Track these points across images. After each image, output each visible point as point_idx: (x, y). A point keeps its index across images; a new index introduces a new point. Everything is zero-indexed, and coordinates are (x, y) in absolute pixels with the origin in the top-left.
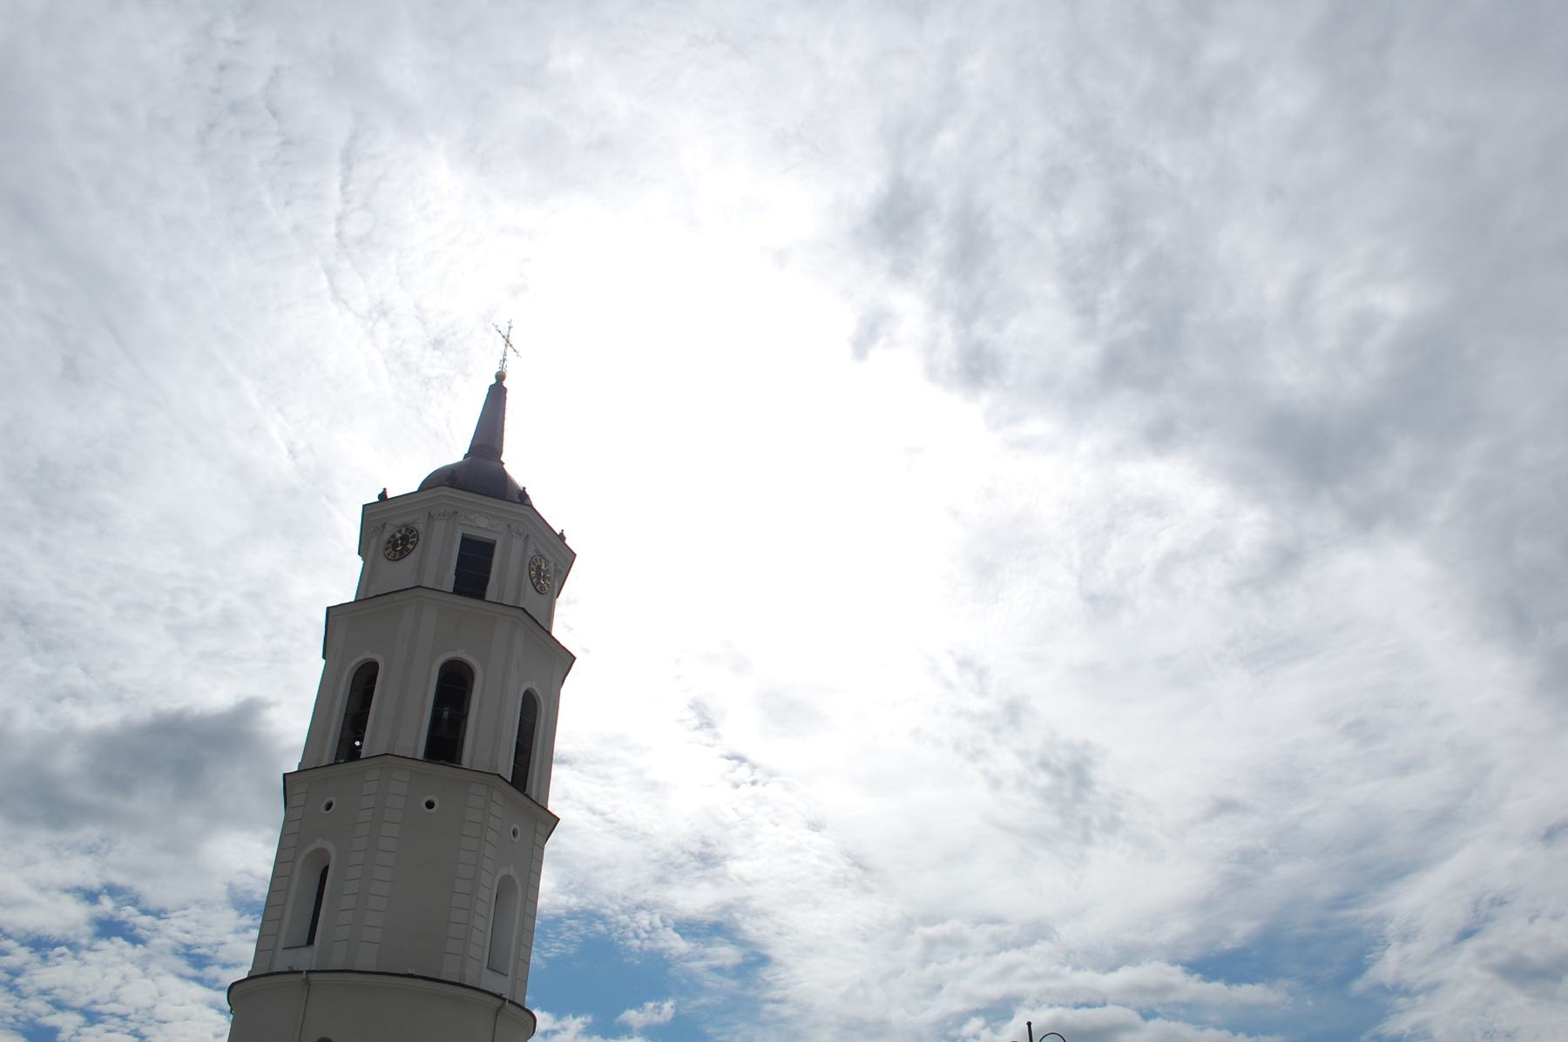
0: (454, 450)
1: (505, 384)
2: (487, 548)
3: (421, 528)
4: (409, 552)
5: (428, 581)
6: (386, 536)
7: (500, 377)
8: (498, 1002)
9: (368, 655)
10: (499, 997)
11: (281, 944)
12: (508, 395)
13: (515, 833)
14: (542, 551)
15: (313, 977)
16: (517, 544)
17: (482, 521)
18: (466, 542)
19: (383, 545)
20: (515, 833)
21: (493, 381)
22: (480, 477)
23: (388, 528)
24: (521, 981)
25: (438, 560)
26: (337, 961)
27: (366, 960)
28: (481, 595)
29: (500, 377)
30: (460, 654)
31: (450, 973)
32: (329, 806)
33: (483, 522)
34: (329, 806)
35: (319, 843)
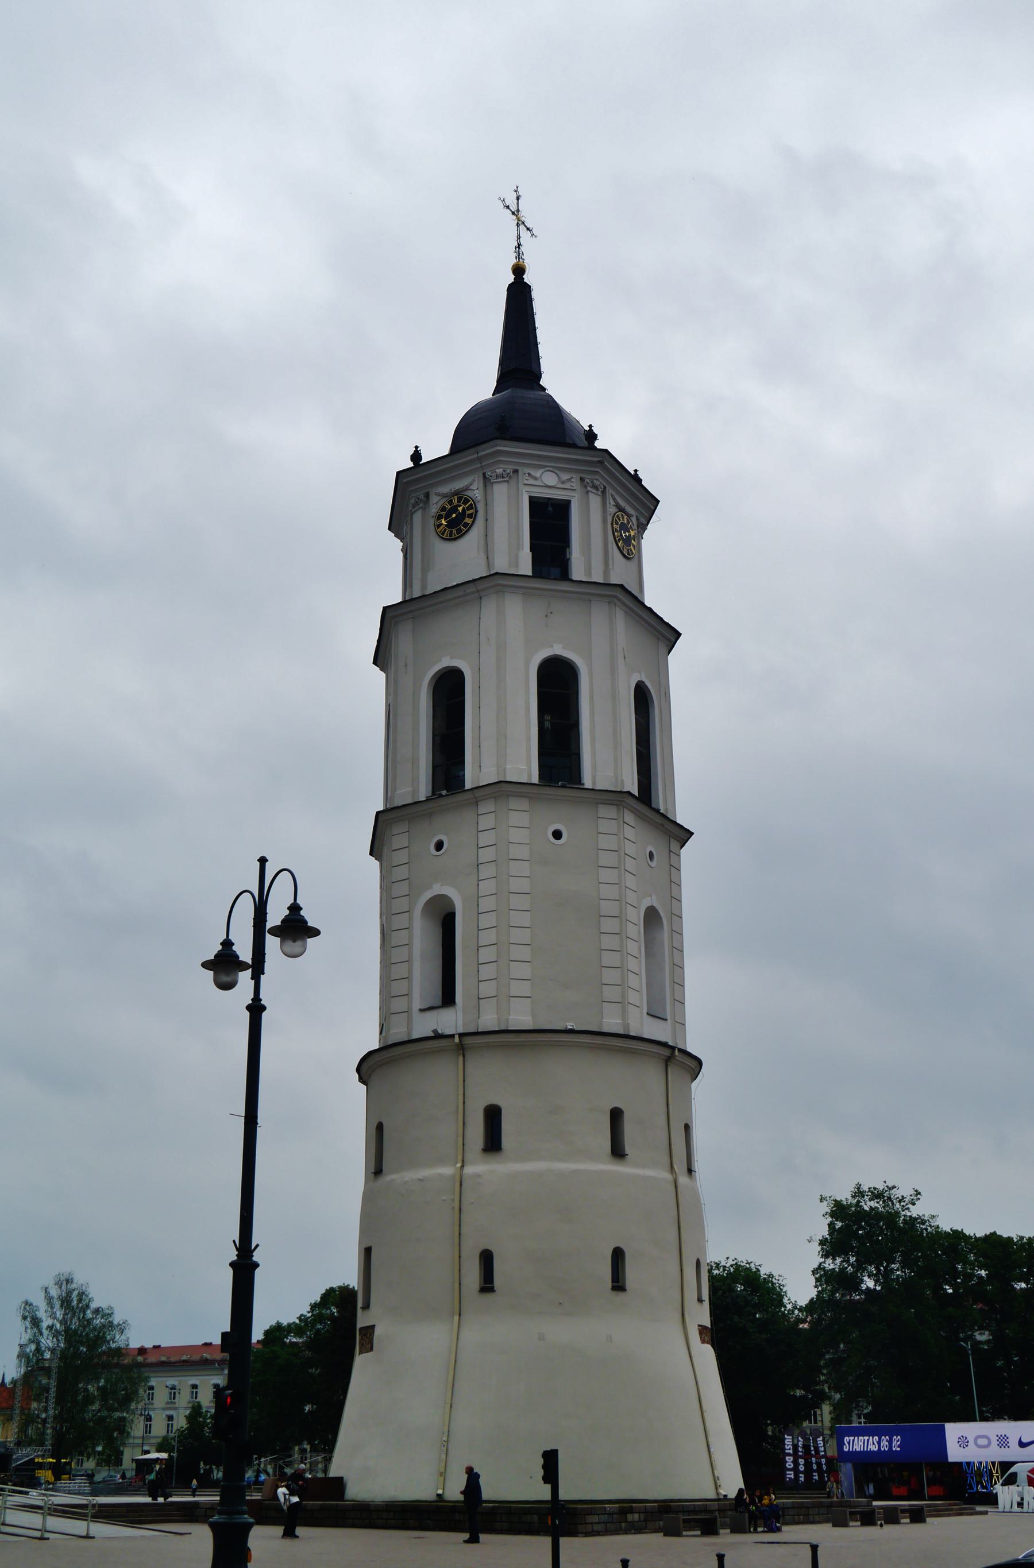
0: (479, 382)
1: (527, 278)
2: (562, 508)
3: (477, 493)
4: (469, 527)
5: (501, 565)
6: (434, 509)
7: (519, 271)
8: (667, 1052)
9: (447, 662)
10: (664, 1045)
11: (417, 1005)
12: (534, 294)
13: (651, 855)
14: (622, 503)
15: (467, 1041)
16: (595, 500)
17: (549, 481)
18: (537, 506)
19: (432, 521)
20: (651, 855)
21: (511, 278)
22: (519, 414)
23: (434, 499)
24: (681, 1024)
25: (505, 537)
26: (489, 1020)
27: (521, 1018)
28: (563, 573)
29: (519, 271)
30: (558, 650)
31: (611, 1023)
32: (439, 846)
33: (550, 479)
34: (439, 846)
35: (437, 889)
